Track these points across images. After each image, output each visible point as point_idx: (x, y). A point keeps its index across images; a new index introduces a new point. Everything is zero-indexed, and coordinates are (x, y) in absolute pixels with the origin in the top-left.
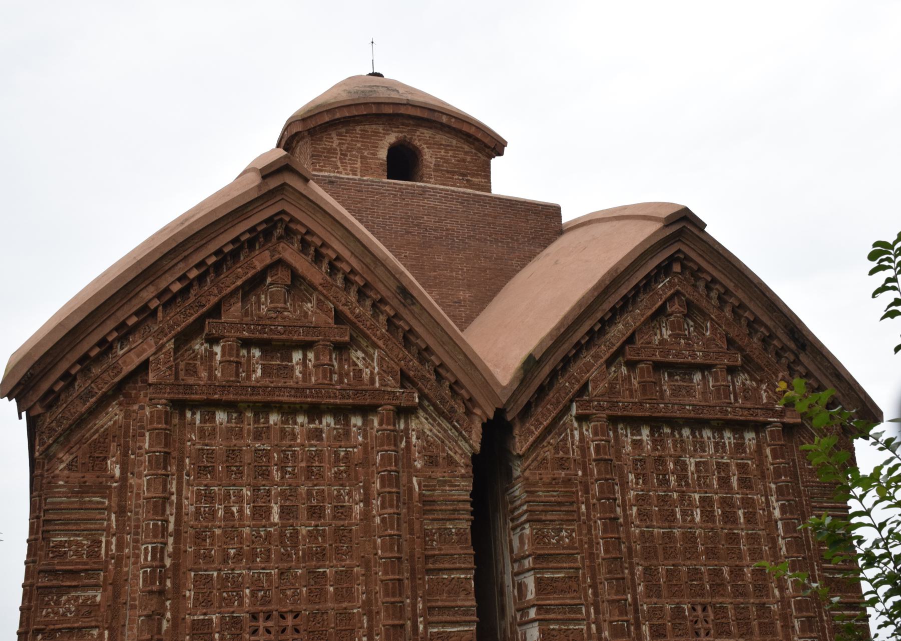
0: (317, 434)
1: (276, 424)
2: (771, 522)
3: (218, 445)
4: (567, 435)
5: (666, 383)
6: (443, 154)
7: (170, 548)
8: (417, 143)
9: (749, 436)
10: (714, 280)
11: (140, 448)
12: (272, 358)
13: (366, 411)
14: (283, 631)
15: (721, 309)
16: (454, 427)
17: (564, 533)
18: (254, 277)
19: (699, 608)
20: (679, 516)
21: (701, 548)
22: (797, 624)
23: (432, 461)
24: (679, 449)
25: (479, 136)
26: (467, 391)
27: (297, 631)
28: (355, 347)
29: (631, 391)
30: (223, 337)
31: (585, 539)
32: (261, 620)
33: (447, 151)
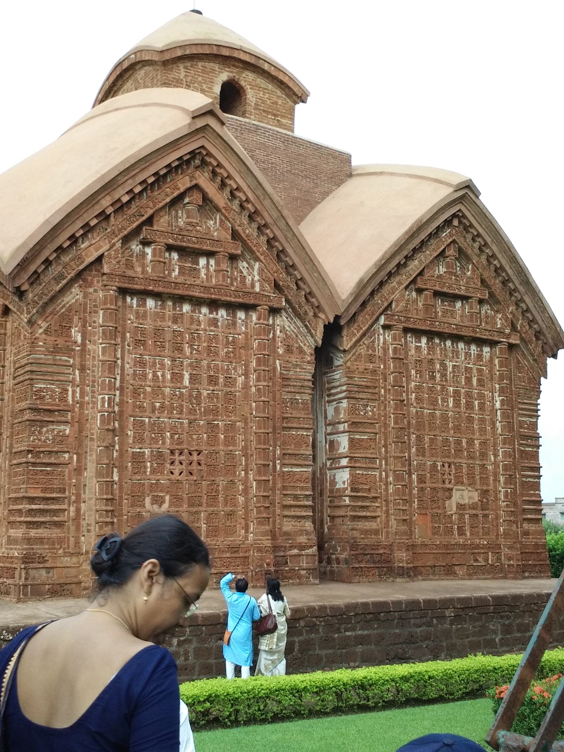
0: (214, 322)
2: (494, 411)
3: (149, 325)
4: (375, 339)
5: (440, 306)
7: (117, 400)
8: (243, 83)
9: (486, 349)
10: (479, 235)
13: (248, 308)
14: (191, 464)
15: (479, 256)
17: (369, 408)
19: (446, 465)
20: (440, 402)
21: (451, 425)
22: (502, 479)
23: (289, 349)
24: (443, 355)
25: (291, 85)
26: (317, 300)
27: (199, 464)
29: (417, 309)
30: (155, 242)
31: (383, 414)
32: (177, 455)
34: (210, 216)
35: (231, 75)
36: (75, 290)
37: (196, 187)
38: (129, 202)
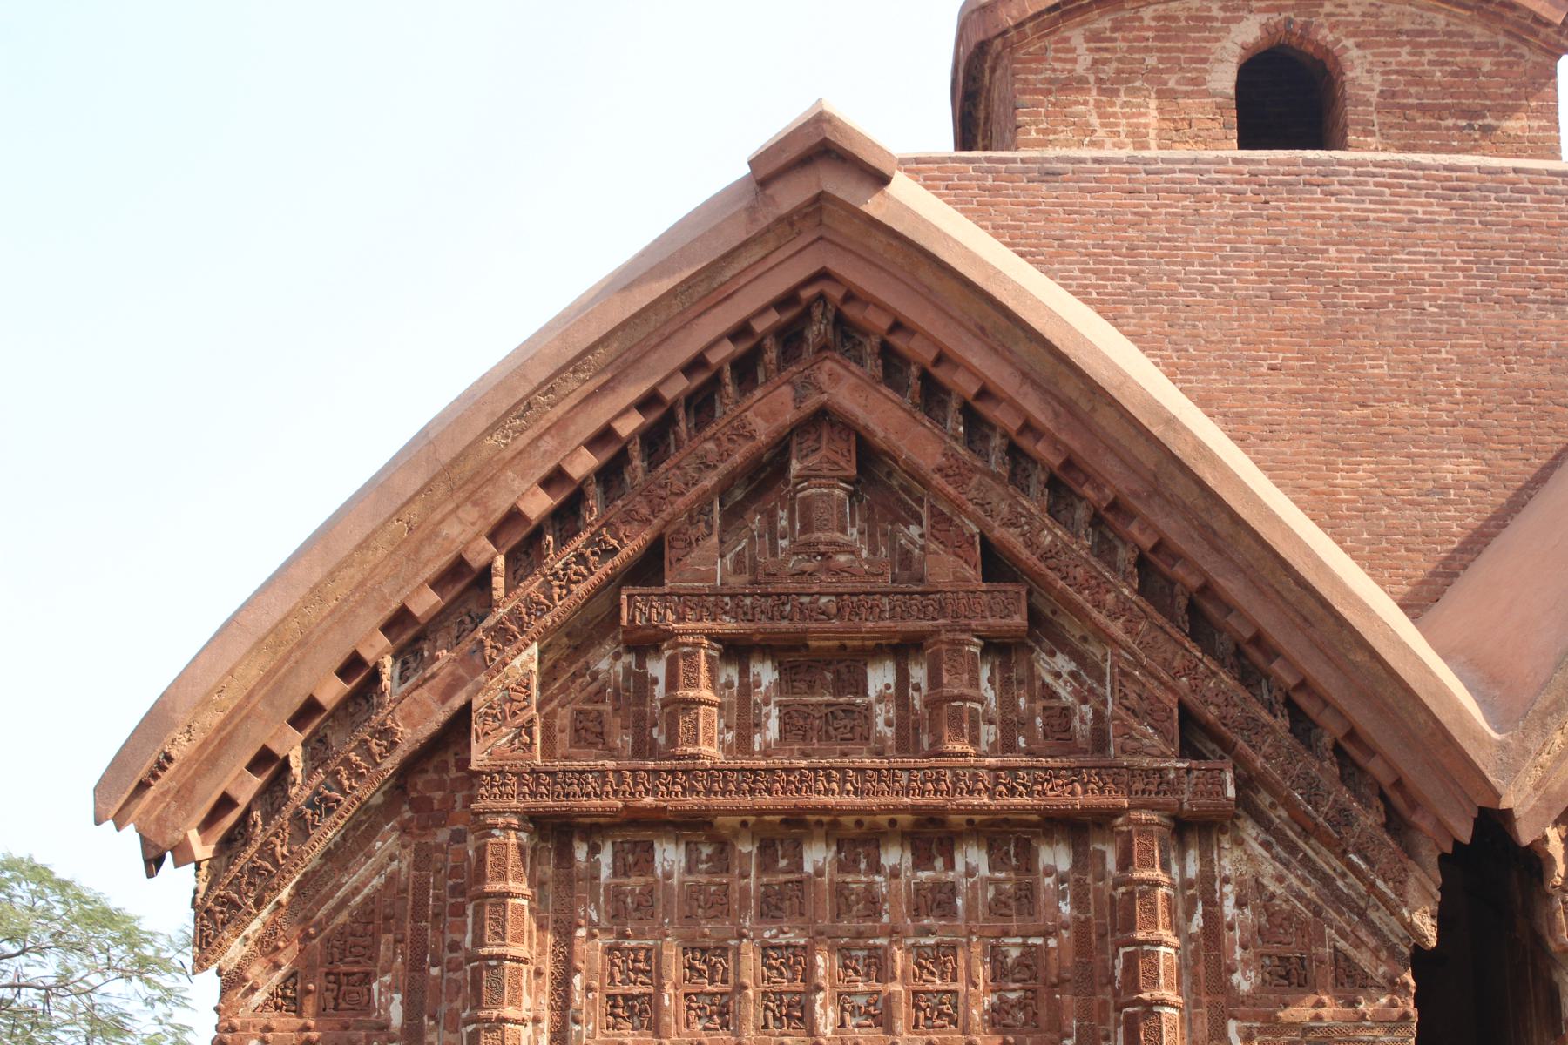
0: (938, 900)
1: (819, 873)
6: (1405, 58)
8: (1325, 35)
11: (455, 946)
12: (811, 689)
16: (1352, 866)
28: (1047, 643)
33: (1417, 49)
34: (908, 509)
35: (1276, 17)
36: (386, 843)
37: (823, 419)
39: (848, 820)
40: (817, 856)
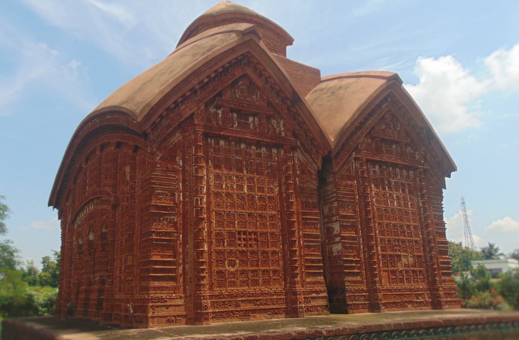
0: (259, 155)
7: (205, 200)
9: (411, 172)
13: (278, 146)
17: (350, 207)
18: (236, 80)
23: (303, 172)
36: (178, 134)
37: (245, 76)
38: (208, 82)
39: (247, 141)
40: (243, 146)
